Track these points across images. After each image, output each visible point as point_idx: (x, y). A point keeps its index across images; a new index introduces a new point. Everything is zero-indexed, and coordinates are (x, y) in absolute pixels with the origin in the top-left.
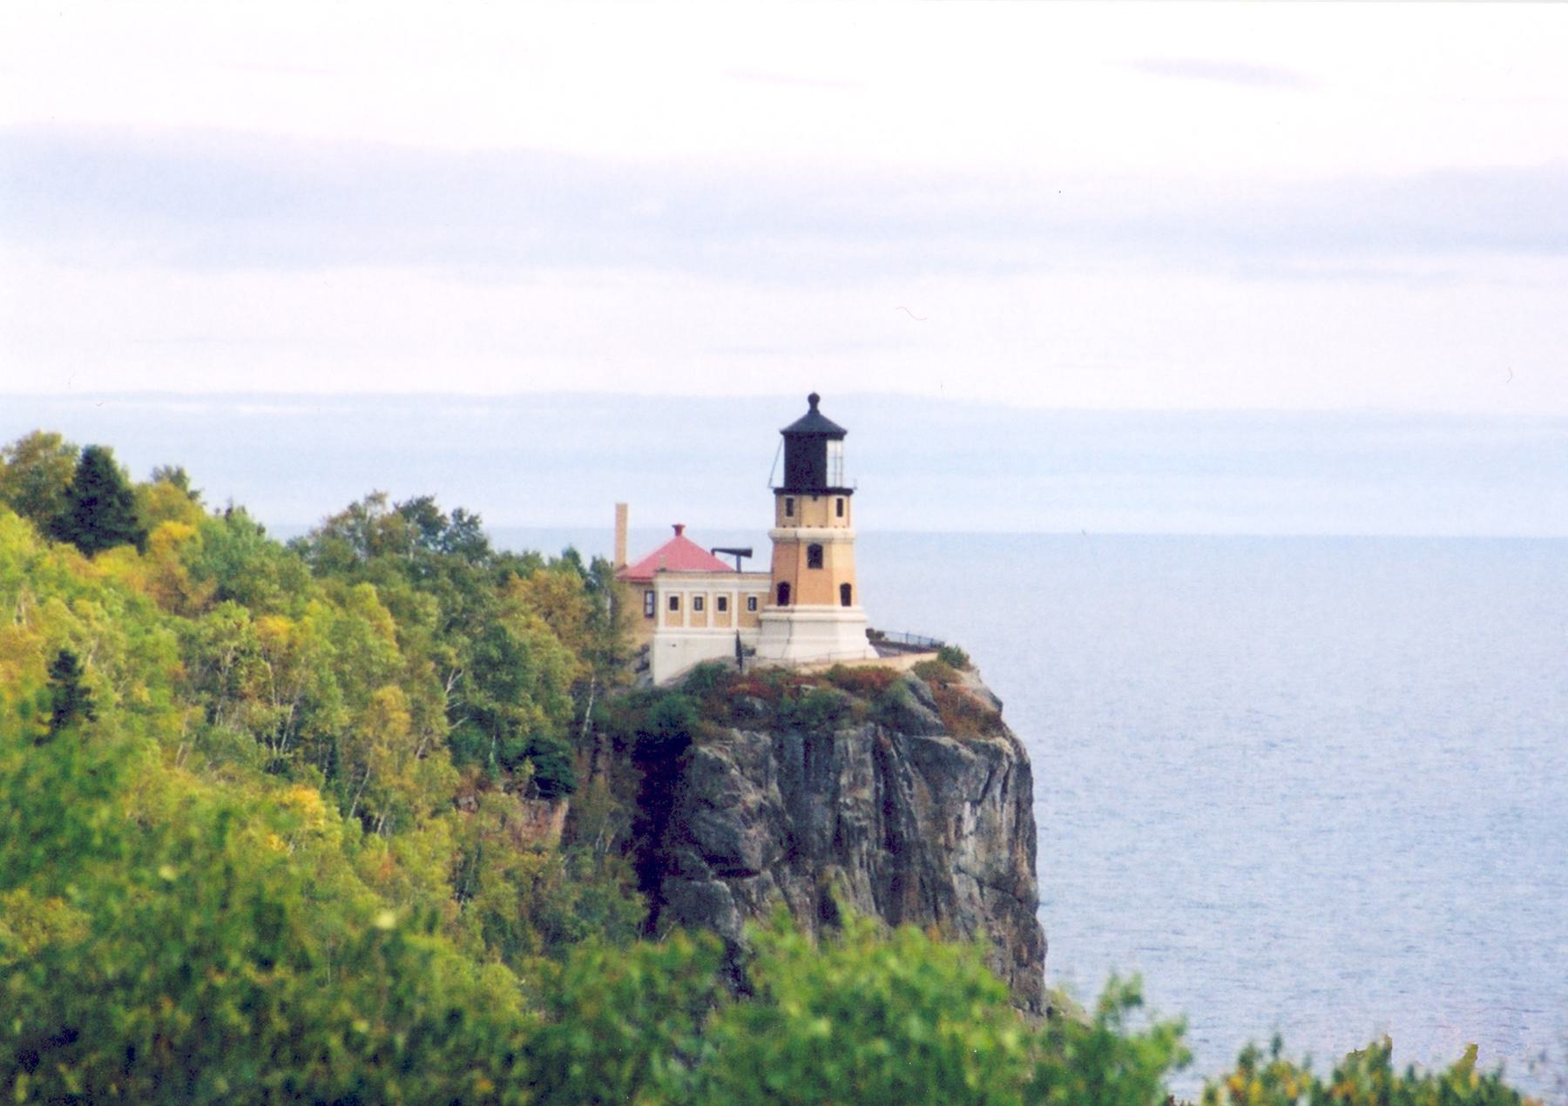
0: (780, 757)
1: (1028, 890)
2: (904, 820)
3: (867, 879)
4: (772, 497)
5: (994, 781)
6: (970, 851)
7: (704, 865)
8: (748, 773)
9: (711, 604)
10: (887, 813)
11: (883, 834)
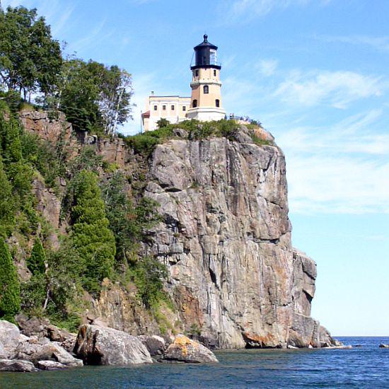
0: (190, 150)
1: (284, 204)
2: (237, 175)
3: (223, 196)
5: (272, 162)
6: (264, 190)
7: (160, 187)
8: (177, 154)
9: (169, 107)
10: (231, 172)
11: (230, 180)
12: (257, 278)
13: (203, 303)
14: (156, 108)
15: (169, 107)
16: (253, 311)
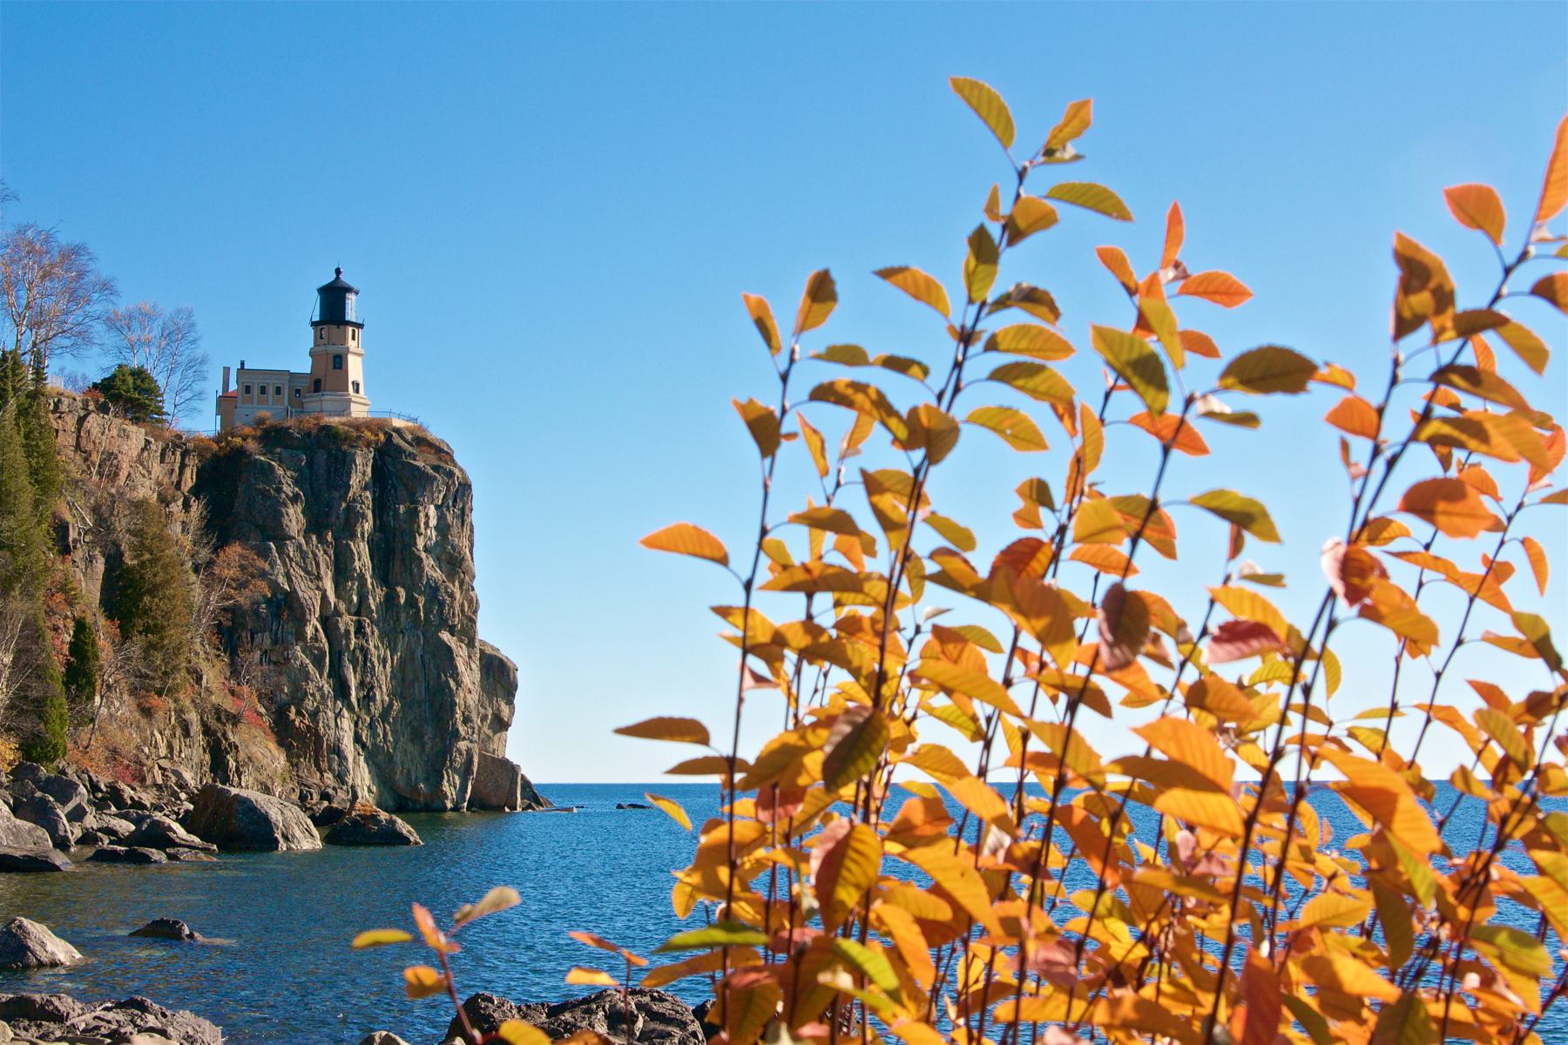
2: (391, 513)
4: (311, 331)
9: (271, 391)
12: (420, 693)
13: (329, 736)
14: (248, 389)
15: (271, 391)
16: (410, 748)
